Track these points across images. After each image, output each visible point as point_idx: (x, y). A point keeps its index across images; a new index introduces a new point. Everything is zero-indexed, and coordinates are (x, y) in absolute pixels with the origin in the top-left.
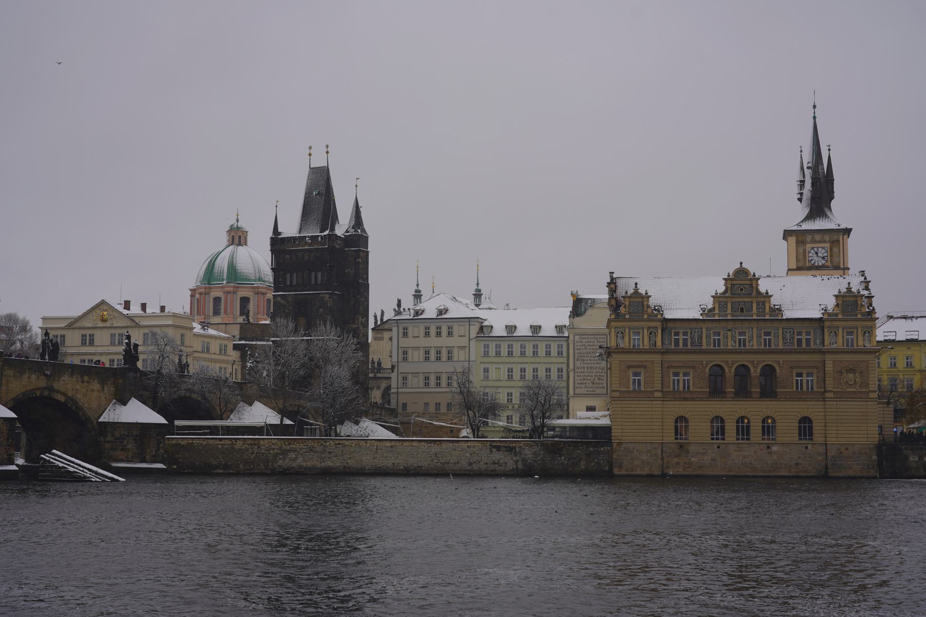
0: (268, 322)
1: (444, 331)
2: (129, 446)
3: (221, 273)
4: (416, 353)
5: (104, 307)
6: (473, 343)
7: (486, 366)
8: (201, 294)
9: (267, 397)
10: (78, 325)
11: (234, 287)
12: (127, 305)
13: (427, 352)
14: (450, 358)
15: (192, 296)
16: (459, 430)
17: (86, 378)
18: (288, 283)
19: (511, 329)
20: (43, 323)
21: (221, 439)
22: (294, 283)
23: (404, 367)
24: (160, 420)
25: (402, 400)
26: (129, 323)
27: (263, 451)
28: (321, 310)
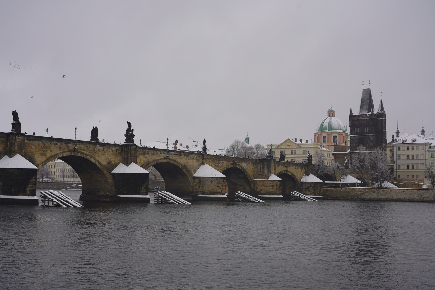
0: (344, 145)
1: (415, 148)
3: (326, 127)
4: (404, 156)
5: (289, 141)
6: (427, 153)
9: (352, 173)
10: (280, 147)
12: (296, 140)
13: (408, 156)
15: (315, 136)
16: (422, 185)
17: (297, 167)
18: (356, 132)
22: (358, 131)
23: (399, 162)
24: (321, 181)
25: (398, 174)
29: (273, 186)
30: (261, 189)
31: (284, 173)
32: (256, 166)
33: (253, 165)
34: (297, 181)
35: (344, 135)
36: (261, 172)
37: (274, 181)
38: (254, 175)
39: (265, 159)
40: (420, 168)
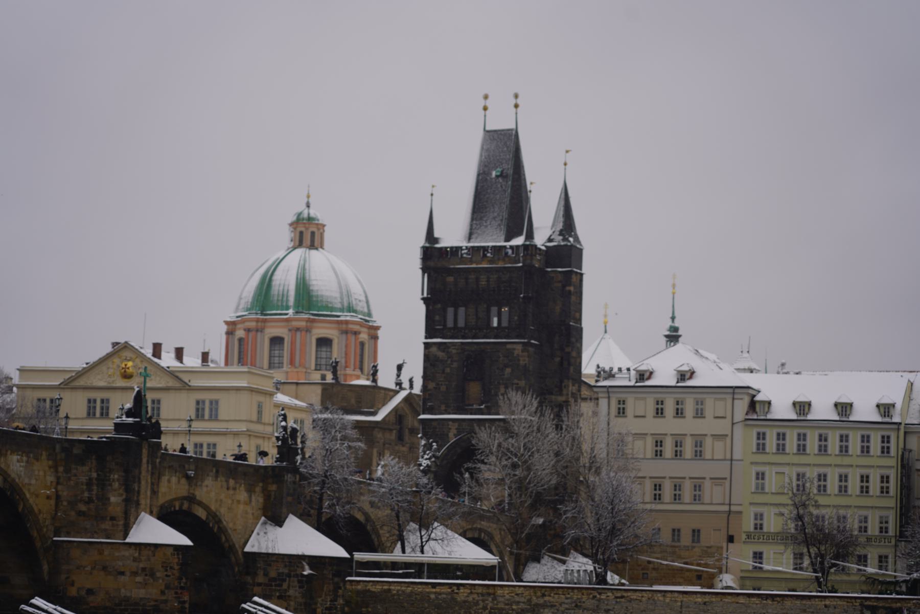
0: (368, 383)
1: (689, 408)
2: (291, 592)
3: (284, 295)
4: (639, 444)
6: (739, 431)
7: (760, 469)
8: (248, 330)
10: (81, 382)
11: (309, 320)
12: (157, 349)
13: (659, 443)
14: (698, 454)
15: (230, 333)
18: (450, 324)
19: (802, 407)
20: (21, 377)
21: (434, 585)
26: (171, 383)
27: (501, 606)
28: (508, 370)
29: (150, 573)
30: (88, 586)
31: (181, 511)
32: (67, 470)
33: (55, 467)
34: (232, 548)
35: (364, 336)
36: (90, 501)
37: (156, 546)
38: (54, 518)
39: (111, 442)
40: (707, 499)
